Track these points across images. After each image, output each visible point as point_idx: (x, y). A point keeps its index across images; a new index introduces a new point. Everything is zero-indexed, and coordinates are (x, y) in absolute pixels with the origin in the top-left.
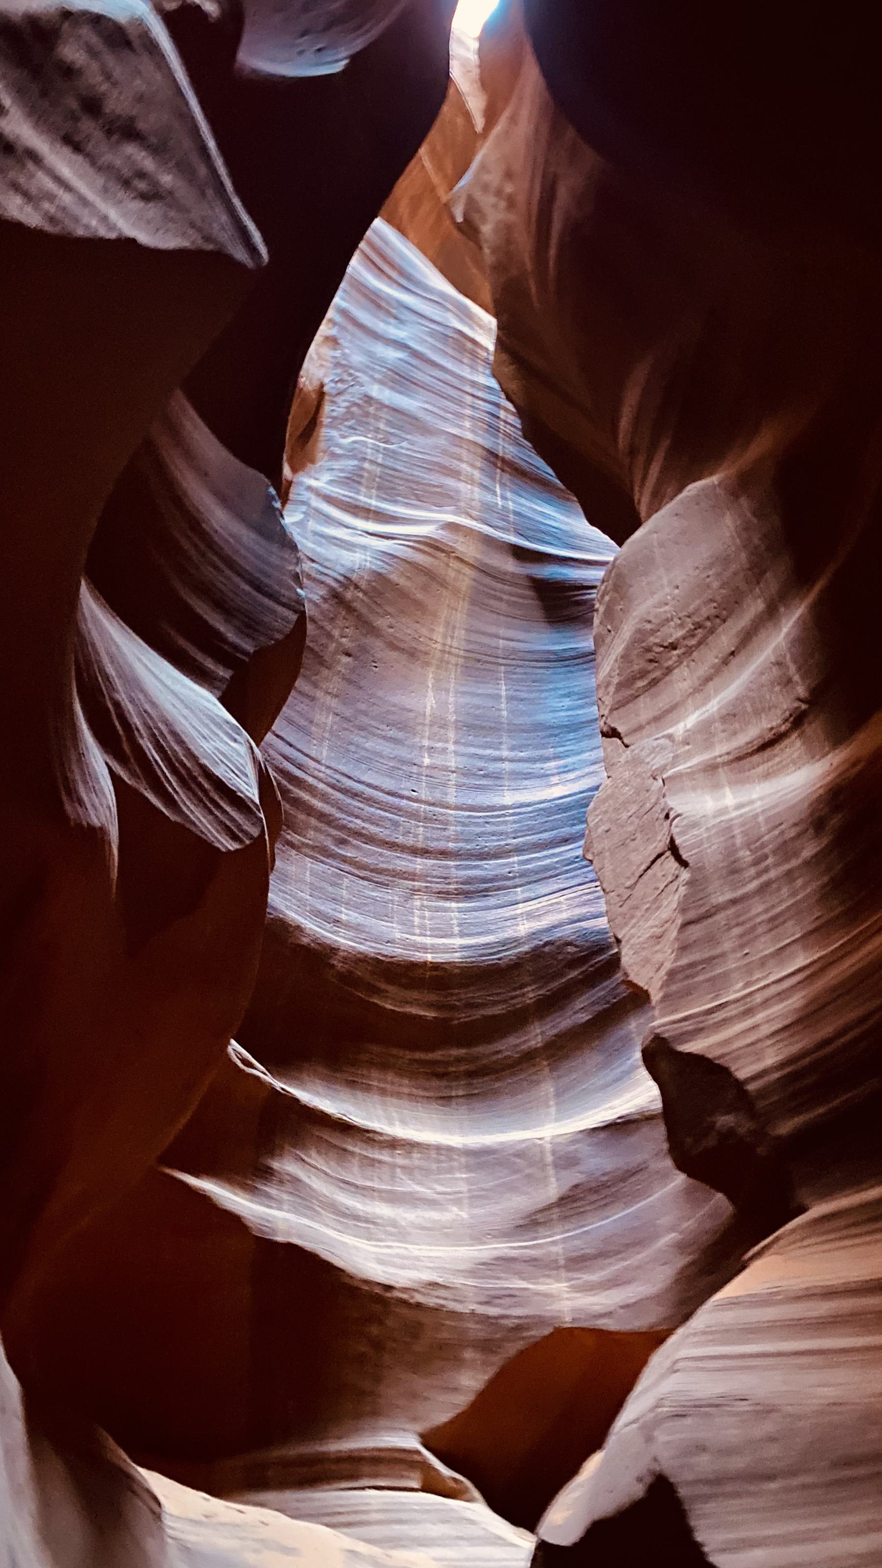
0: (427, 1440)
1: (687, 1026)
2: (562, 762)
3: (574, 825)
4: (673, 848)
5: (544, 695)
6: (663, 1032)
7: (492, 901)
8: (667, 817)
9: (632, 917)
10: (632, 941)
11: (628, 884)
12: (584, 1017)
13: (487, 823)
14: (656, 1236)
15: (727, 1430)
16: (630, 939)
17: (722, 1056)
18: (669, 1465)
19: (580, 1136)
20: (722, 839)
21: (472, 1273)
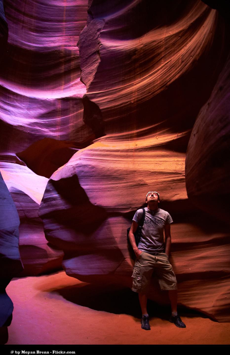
0: (17, 155)
1: (93, 96)
3: (68, 17)
6: (89, 96)
7: (43, 35)
8: (99, 44)
9: (85, 66)
10: (84, 72)
11: (86, 57)
13: (45, 9)
15: (86, 169)
16: (84, 71)
17: (99, 103)
19: (56, 100)
20: (110, 54)
21: (29, 125)
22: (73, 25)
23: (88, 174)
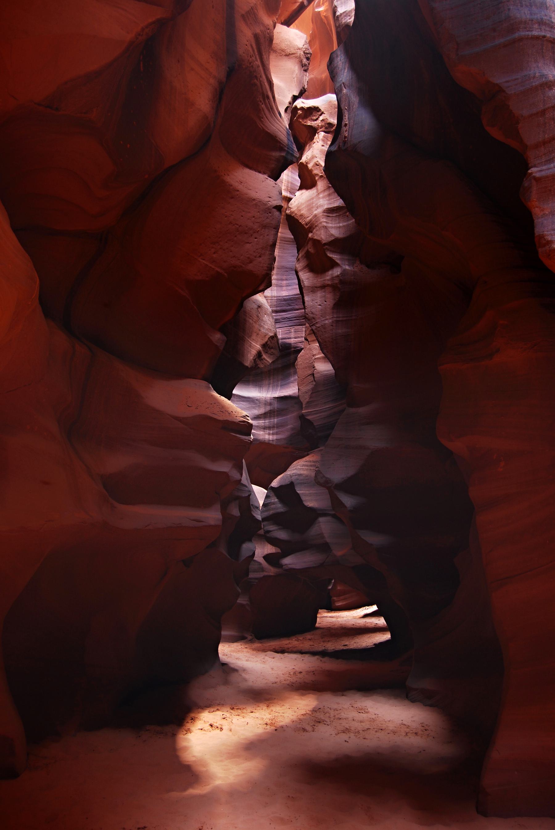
2: (287, 282)
4: (313, 374)
5: (286, 255)
12: (280, 366)
14: (288, 425)
15: (301, 478)
18: (293, 481)
22: (293, 314)
23: (302, 481)
